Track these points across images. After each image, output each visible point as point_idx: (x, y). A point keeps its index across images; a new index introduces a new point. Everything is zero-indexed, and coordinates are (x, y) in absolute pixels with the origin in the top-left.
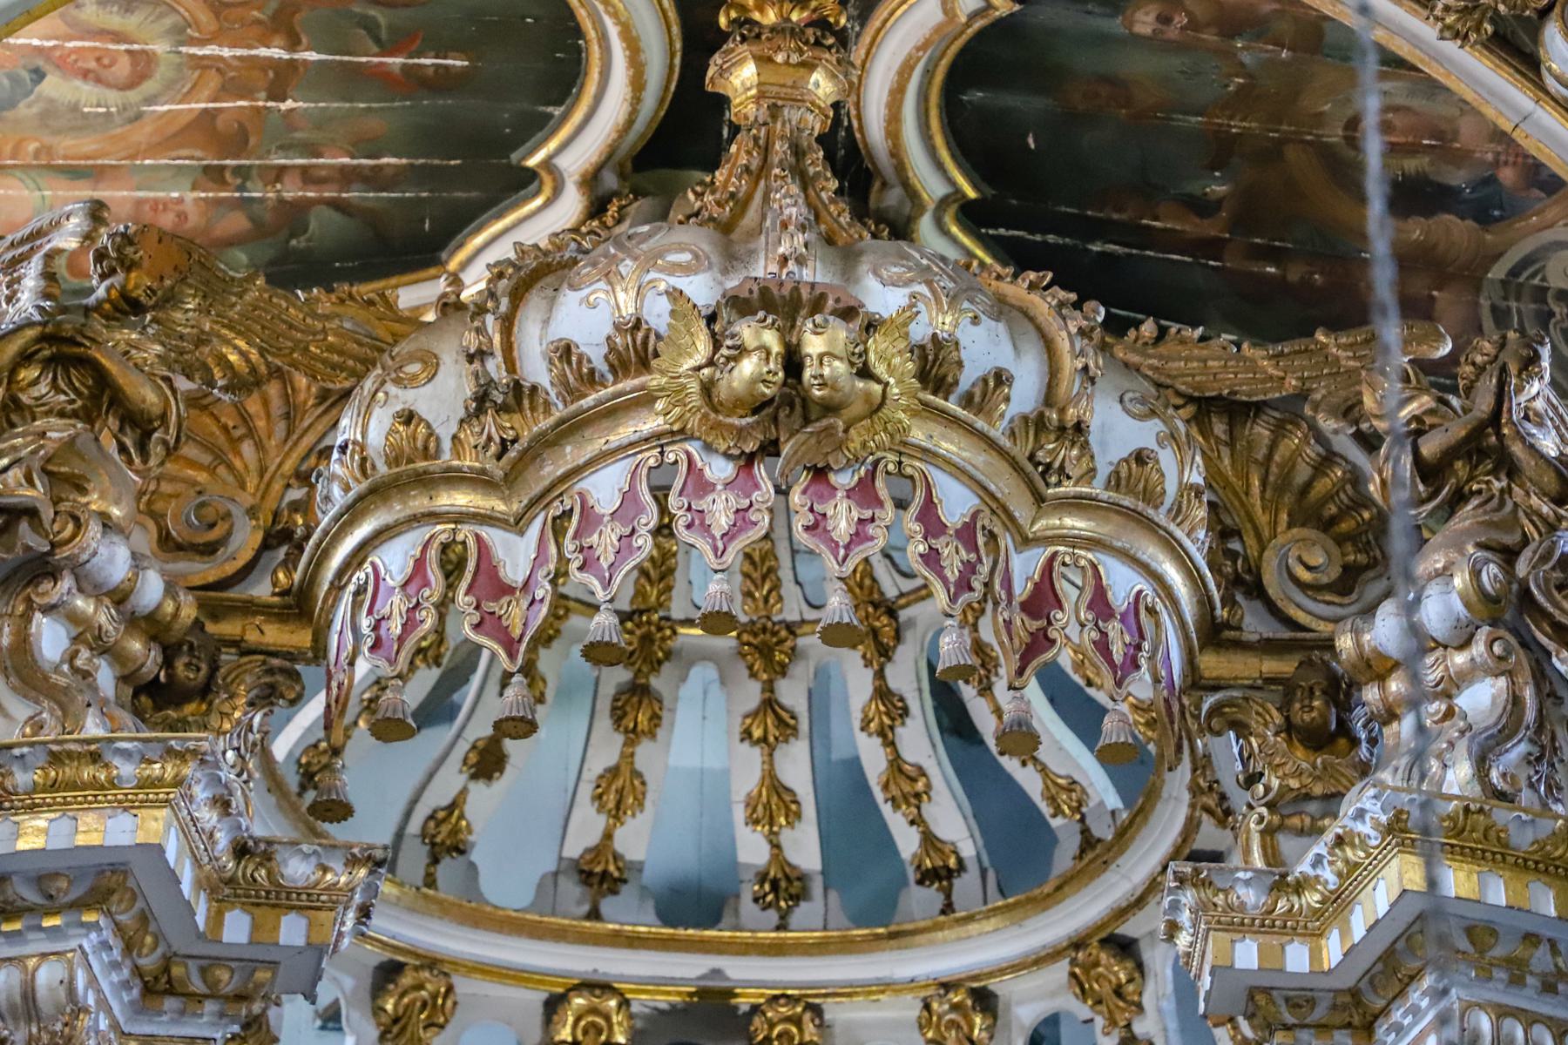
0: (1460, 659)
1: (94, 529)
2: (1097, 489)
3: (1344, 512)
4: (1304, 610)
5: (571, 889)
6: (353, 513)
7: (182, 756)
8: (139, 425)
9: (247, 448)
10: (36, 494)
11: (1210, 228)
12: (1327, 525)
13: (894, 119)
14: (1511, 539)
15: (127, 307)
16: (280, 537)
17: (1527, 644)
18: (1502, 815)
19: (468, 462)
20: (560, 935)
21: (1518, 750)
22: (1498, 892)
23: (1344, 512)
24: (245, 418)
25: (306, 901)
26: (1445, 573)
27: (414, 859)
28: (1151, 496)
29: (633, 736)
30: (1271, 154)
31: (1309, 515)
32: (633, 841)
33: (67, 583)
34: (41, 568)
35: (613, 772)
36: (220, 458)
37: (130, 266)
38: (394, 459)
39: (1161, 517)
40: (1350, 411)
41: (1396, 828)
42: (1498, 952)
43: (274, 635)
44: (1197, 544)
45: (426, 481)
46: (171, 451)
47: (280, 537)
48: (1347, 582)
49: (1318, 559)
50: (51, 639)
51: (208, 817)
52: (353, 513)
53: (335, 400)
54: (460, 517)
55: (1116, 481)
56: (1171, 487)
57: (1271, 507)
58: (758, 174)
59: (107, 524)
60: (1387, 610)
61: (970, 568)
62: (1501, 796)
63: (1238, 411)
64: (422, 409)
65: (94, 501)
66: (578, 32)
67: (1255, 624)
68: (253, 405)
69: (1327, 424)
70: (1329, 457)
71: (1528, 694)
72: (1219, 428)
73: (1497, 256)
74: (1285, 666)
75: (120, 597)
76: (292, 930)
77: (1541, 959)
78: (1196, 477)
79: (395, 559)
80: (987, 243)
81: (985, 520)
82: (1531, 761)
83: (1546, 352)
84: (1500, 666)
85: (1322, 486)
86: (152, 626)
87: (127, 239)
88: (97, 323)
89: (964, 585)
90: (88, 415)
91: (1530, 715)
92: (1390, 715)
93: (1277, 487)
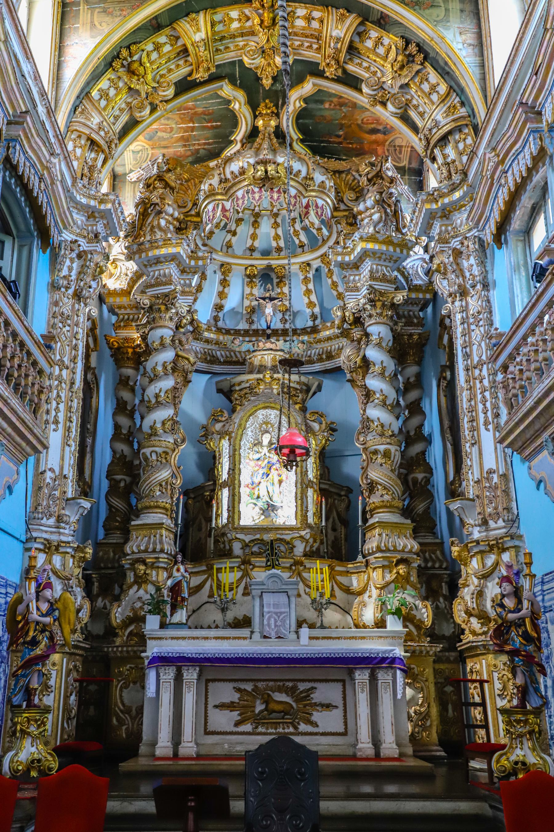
0: (373, 211)
1: (167, 206)
2: (316, 188)
3: (357, 188)
4: (350, 204)
5: (248, 252)
6: (204, 200)
7: (182, 239)
8: (172, 189)
9: (189, 191)
10: (158, 201)
11: (340, 140)
12: (354, 190)
13: (288, 126)
14: (382, 191)
15: (169, 170)
16: (195, 204)
17: (383, 207)
18: (378, 235)
19: (220, 191)
20: (246, 259)
21: (381, 224)
22: (377, 247)
23: (357, 188)
24: (189, 186)
25: (202, 258)
26: (371, 197)
27: (225, 249)
28: (325, 188)
29: (255, 228)
30: (350, 126)
31: (352, 189)
32: (256, 244)
33: (164, 214)
34: (160, 212)
35: (253, 234)
36: (185, 192)
37: (169, 164)
38: (209, 192)
39: (326, 191)
40: (358, 171)
41: (361, 238)
42: (377, 256)
43: (195, 219)
44: (333, 195)
45: (214, 195)
46: (177, 193)
47: (195, 204)
48: (357, 199)
49: (352, 196)
50: (163, 223)
51: (187, 247)
52: (204, 200)
53: (201, 182)
54: (219, 200)
55: (319, 186)
56: (328, 187)
57: (345, 187)
58: (263, 139)
59: (168, 205)
60: (362, 203)
61: (296, 202)
62: (378, 232)
63: (340, 172)
64: (213, 183)
65: (167, 201)
66: (236, 117)
67: (342, 207)
68: (190, 184)
69: (354, 173)
70: (355, 179)
71: (383, 216)
72: (337, 175)
73: (387, 141)
74: (346, 213)
75: (172, 215)
76: (200, 263)
77: (384, 257)
78: (332, 184)
79: (210, 207)
80: (304, 145)
81: (298, 194)
82: (384, 226)
83: (390, 158)
84: (379, 211)
85: (354, 183)
86: (177, 219)
87: (168, 160)
88: (165, 174)
89: (295, 205)
90: (165, 188)
91: (383, 219)
92: (362, 220)
93: (346, 185)
